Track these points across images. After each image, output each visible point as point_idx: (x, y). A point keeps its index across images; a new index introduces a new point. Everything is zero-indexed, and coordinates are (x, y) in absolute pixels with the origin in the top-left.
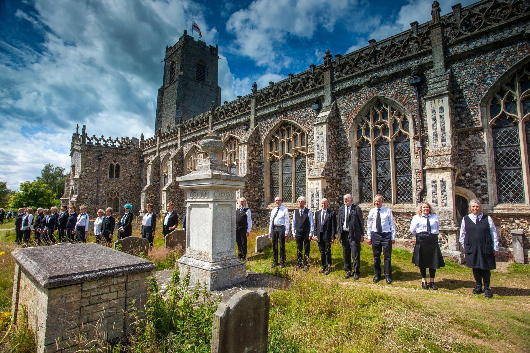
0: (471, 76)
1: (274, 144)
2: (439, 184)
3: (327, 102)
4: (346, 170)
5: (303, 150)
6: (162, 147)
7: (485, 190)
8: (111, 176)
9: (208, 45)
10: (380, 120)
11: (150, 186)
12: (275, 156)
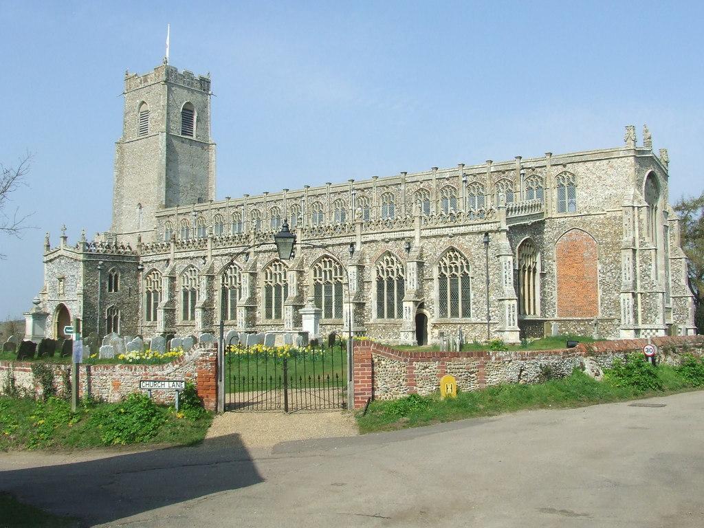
0: (431, 249)
1: (318, 271)
2: (408, 309)
3: (357, 248)
4: (370, 297)
5: (341, 279)
6: (178, 256)
7: (433, 312)
8: (110, 290)
9: (197, 77)
10: (390, 265)
11: (168, 302)
12: (319, 281)
